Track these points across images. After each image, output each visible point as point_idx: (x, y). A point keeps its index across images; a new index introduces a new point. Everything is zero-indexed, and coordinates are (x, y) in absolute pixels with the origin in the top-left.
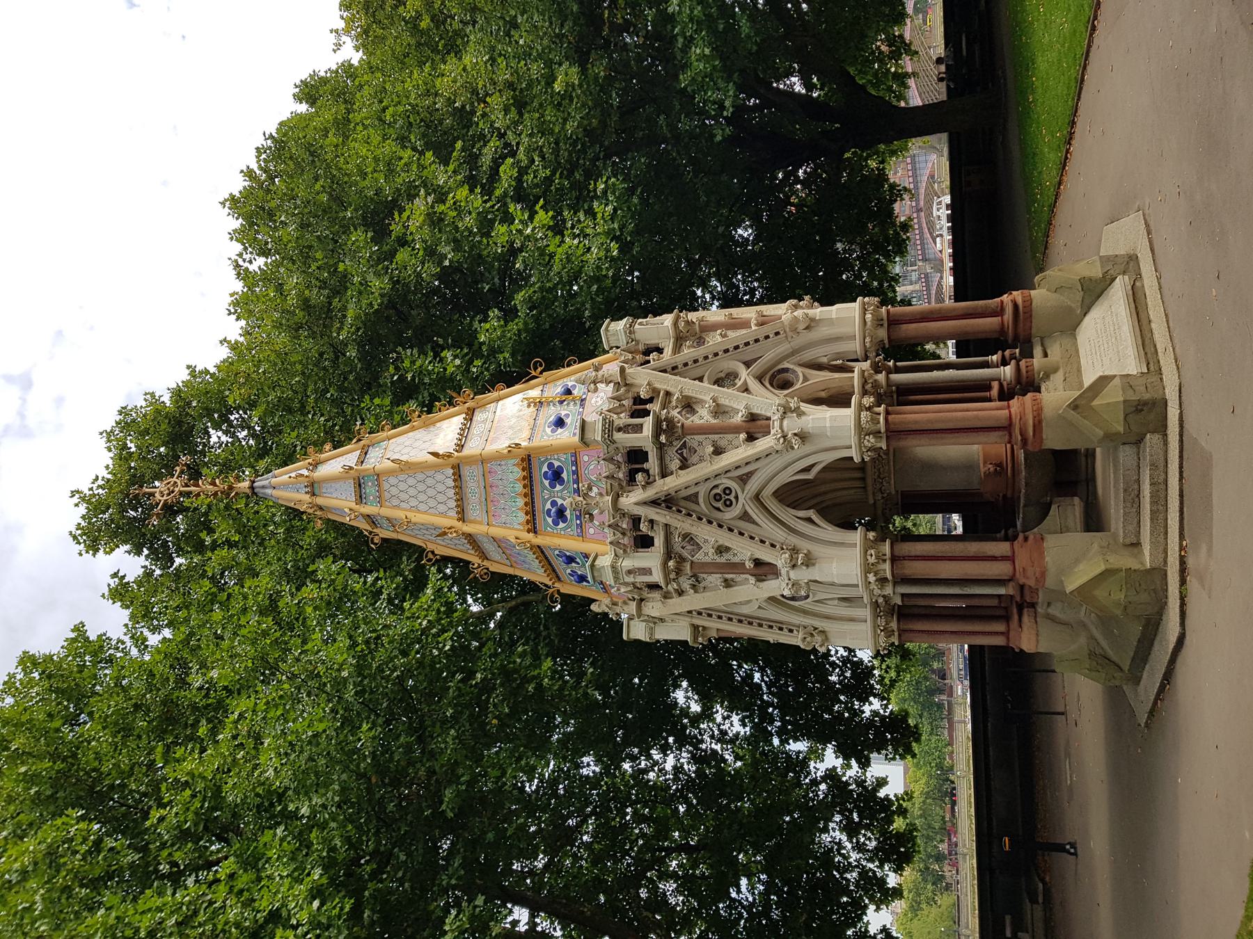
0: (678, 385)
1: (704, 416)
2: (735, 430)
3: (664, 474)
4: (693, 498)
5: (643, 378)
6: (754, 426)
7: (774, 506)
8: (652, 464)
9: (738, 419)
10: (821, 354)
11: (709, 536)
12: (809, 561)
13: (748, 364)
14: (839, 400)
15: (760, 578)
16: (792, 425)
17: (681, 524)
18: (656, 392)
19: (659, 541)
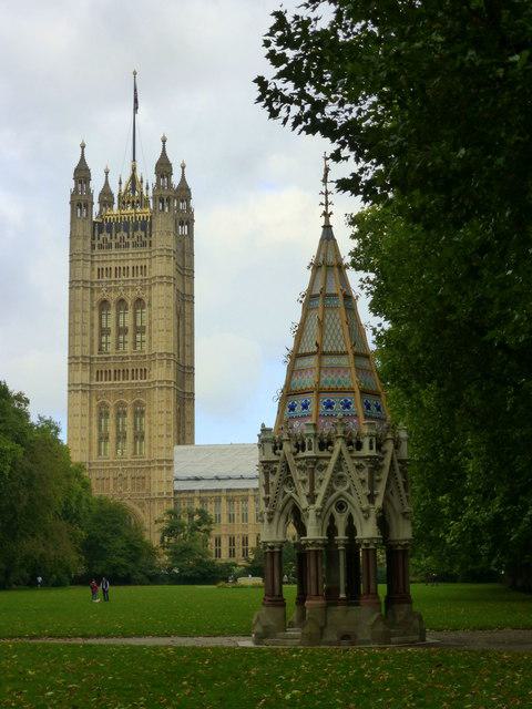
0: (332, 463)
1: (318, 475)
2: (312, 488)
3: (297, 460)
4: (289, 471)
5: (339, 445)
6: (312, 498)
7: (291, 504)
8: (301, 454)
9: (316, 492)
10: (356, 522)
11: (274, 479)
12: (270, 520)
13: (349, 490)
14: (332, 531)
15: (264, 499)
16: (312, 513)
17: (278, 467)
18: (332, 452)
19: (275, 458)
